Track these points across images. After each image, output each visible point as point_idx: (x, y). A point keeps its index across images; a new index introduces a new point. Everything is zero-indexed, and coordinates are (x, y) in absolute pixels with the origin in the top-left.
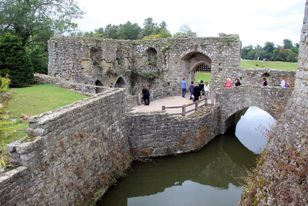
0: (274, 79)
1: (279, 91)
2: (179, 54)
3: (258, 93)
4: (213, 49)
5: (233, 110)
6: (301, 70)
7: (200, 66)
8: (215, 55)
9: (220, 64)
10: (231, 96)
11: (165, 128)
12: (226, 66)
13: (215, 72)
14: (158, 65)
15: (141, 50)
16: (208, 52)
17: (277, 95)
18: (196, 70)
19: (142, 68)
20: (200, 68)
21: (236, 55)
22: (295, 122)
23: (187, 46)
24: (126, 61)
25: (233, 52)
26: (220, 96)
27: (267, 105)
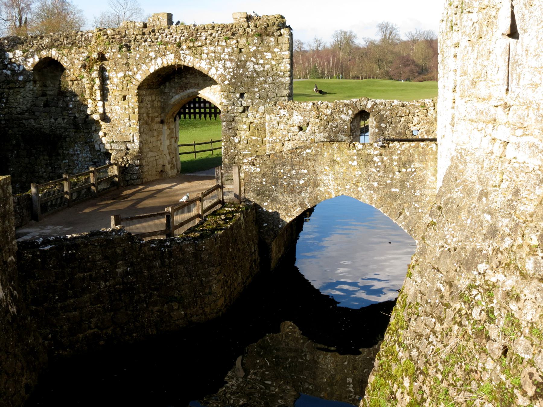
0: (383, 125)
1: (399, 152)
2: (130, 73)
3: (350, 163)
4: (222, 56)
5: (292, 210)
6: (468, 99)
8: (230, 72)
9: (242, 95)
10: (284, 174)
11: (126, 273)
13: (231, 116)
14: (71, 106)
16: (210, 64)
18: (179, 114)
19: (27, 115)
20: (190, 108)
21: (282, 68)
23: (151, 51)
25: (274, 62)
26: (255, 177)
27: (374, 190)
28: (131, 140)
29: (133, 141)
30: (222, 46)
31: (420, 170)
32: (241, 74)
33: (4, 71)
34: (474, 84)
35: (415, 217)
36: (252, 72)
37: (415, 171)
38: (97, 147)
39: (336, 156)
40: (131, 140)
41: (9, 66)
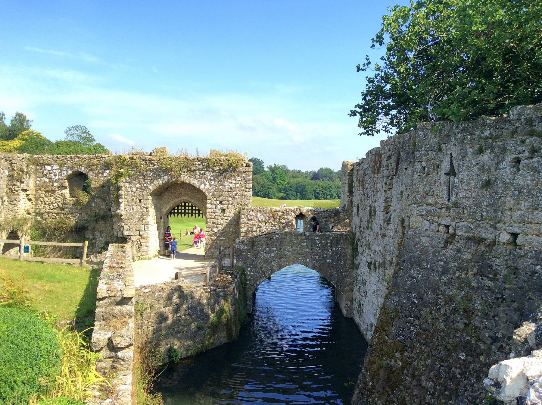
1: (331, 238)
3: (302, 244)
5: (266, 273)
7: (178, 206)
10: (261, 250)
12: (232, 204)
14: (93, 205)
15: (55, 175)
17: (329, 245)
18: (171, 213)
20: (178, 209)
22: (429, 266)
24: (21, 198)
26: (243, 252)
27: (316, 260)
28: (143, 229)
29: (144, 230)
30: (209, 171)
31: (344, 249)
32: (221, 189)
33: (43, 179)
34: (424, 197)
35: (341, 277)
36: (228, 188)
37: (341, 250)
38: (115, 234)
39: (293, 239)
40: (143, 229)
41: (47, 176)
